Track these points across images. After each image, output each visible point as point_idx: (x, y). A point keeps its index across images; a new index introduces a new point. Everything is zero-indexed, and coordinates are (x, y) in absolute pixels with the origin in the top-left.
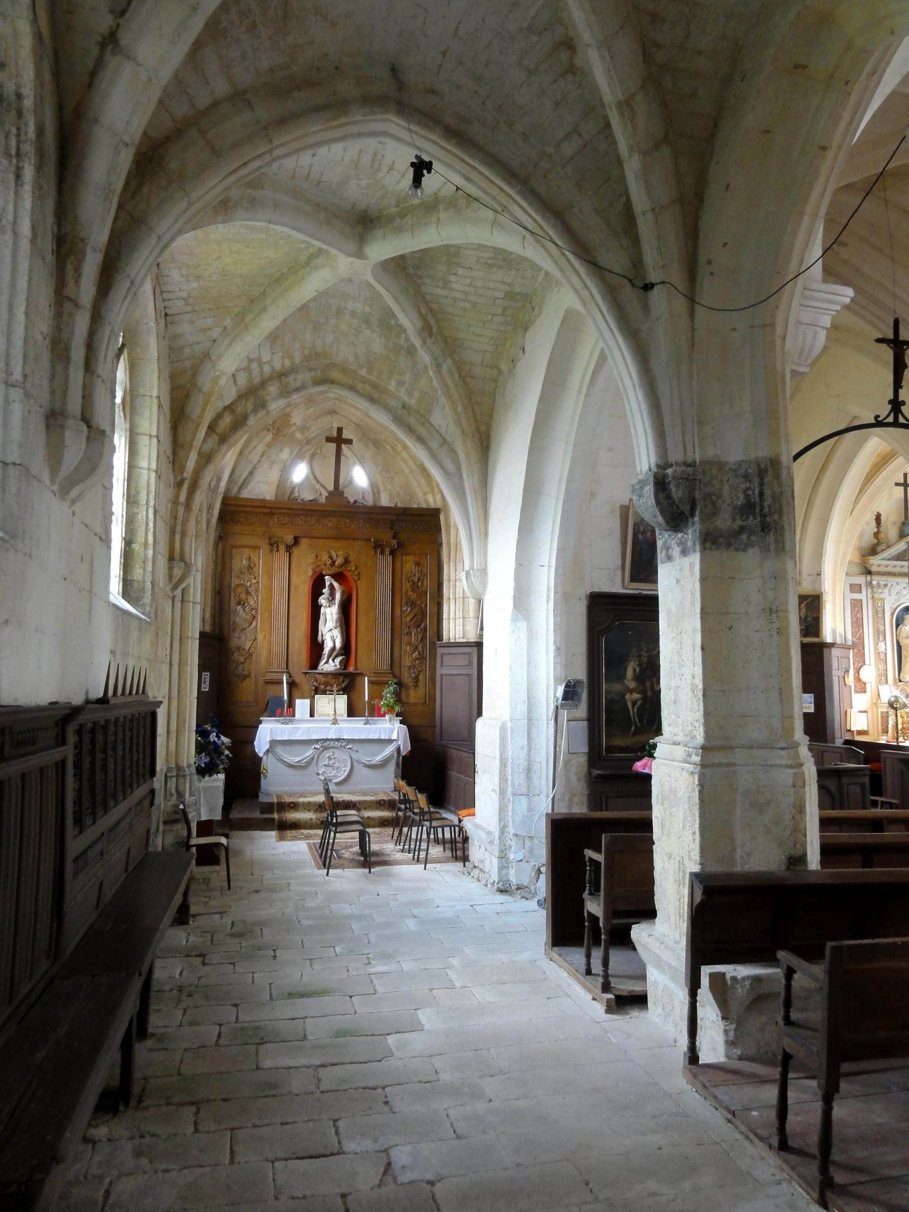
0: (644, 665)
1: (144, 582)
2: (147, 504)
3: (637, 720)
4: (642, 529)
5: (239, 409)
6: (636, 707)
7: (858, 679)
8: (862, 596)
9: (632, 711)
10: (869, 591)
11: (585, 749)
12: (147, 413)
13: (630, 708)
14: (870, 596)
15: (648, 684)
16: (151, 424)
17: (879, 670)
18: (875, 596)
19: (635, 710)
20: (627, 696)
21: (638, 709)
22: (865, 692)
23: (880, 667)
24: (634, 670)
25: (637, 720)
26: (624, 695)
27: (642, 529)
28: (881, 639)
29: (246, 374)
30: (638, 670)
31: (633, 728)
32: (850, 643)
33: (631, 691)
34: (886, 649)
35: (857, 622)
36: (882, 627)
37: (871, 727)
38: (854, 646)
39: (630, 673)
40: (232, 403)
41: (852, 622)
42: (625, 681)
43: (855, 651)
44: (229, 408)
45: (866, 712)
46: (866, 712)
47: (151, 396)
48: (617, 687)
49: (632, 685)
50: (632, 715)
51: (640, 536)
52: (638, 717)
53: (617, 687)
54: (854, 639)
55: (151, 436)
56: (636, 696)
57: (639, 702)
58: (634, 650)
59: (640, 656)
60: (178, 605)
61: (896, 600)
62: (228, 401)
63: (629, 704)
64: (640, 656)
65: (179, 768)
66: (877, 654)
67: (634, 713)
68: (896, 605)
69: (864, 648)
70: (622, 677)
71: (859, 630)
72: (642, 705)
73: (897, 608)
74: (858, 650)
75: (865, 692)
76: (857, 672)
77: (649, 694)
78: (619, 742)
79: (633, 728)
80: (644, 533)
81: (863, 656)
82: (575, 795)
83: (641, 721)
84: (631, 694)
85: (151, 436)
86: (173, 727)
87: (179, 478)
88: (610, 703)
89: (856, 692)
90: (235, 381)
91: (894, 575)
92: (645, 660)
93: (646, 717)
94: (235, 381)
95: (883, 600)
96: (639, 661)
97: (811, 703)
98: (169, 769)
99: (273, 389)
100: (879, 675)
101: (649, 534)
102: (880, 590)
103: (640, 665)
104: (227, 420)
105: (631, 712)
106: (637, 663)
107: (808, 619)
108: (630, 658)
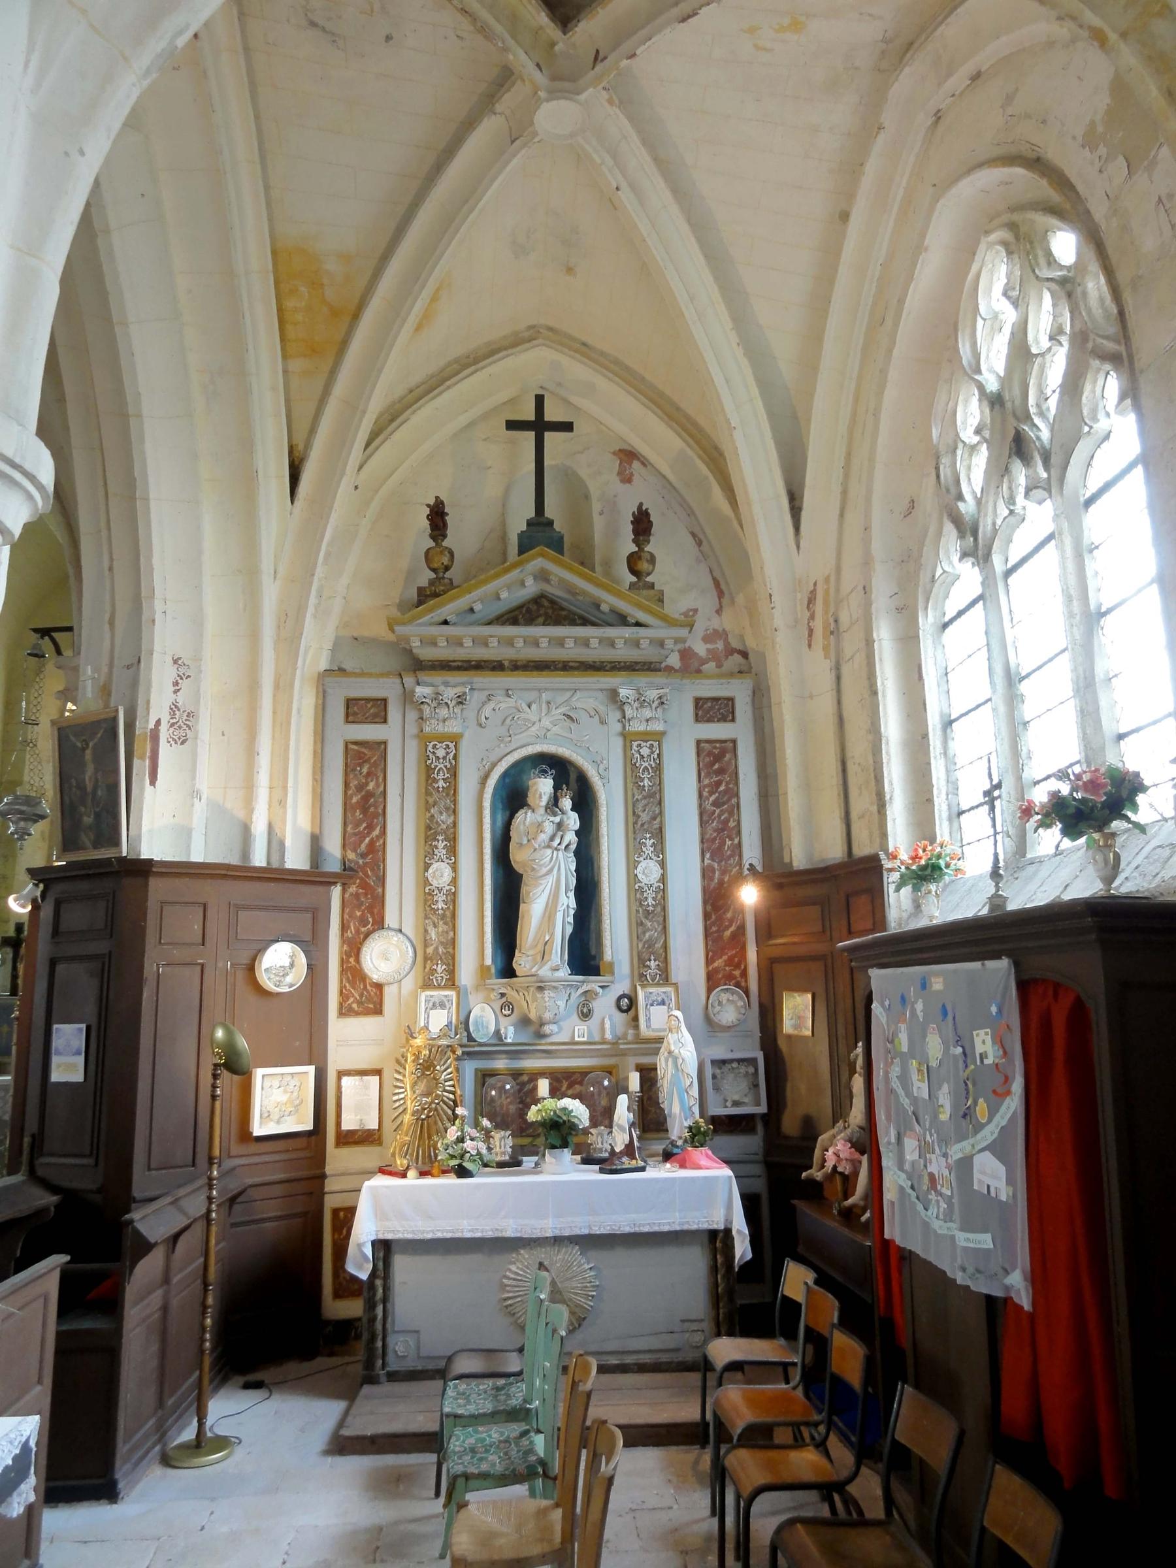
7: (353, 972)
8: (388, 732)
10: (412, 715)
14: (412, 729)
17: (426, 945)
18: (427, 729)
22: (378, 1011)
23: (433, 934)
28: (441, 851)
32: (333, 865)
34: (454, 881)
35: (364, 805)
36: (445, 819)
37: (388, 1127)
38: (348, 873)
41: (347, 807)
43: (353, 889)
45: (378, 1072)
46: (378, 1072)
54: (351, 855)
61: (500, 739)
66: (427, 895)
68: (493, 758)
69: (382, 880)
71: (370, 828)
73: (494, 765)
74: (364, 885)
75: (378, 1011)
76: (353, 949)
81: (378, 902)
89: (345, 1011)
91: (497, 667)
95: (456, 739)
97: (78, 1053)
100: (426, 958)
102: (443, 712)
107: (99, 793)
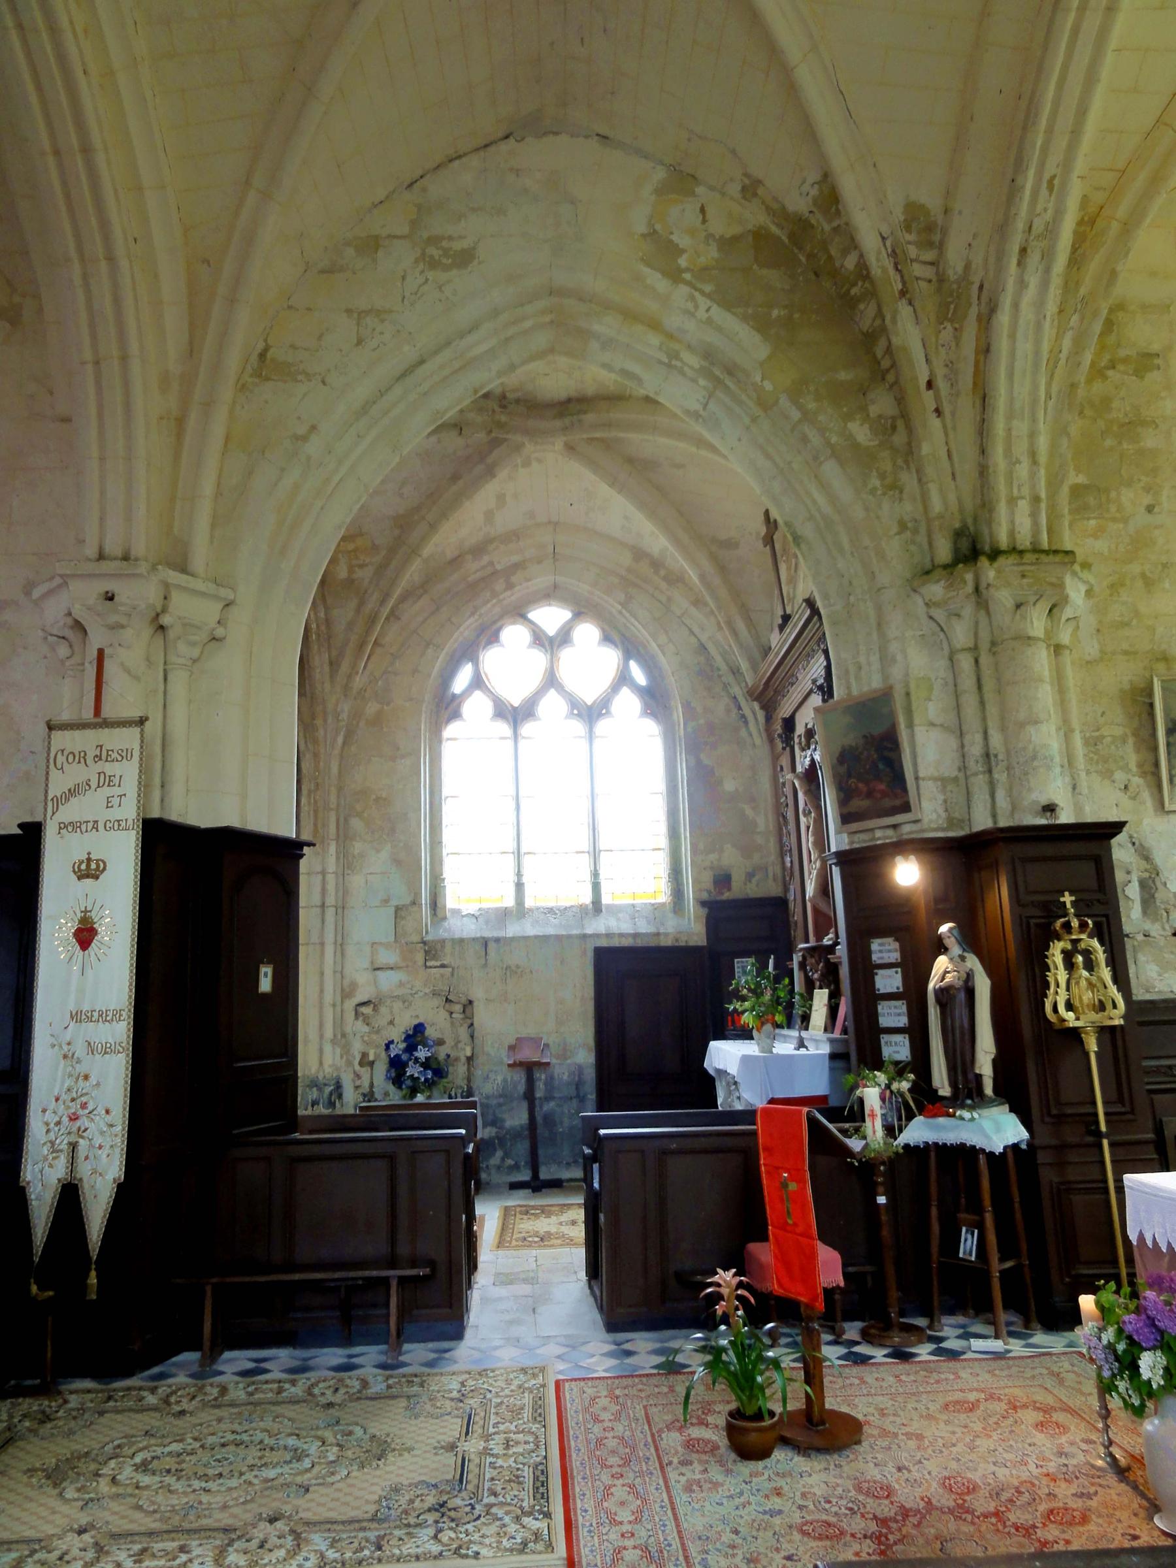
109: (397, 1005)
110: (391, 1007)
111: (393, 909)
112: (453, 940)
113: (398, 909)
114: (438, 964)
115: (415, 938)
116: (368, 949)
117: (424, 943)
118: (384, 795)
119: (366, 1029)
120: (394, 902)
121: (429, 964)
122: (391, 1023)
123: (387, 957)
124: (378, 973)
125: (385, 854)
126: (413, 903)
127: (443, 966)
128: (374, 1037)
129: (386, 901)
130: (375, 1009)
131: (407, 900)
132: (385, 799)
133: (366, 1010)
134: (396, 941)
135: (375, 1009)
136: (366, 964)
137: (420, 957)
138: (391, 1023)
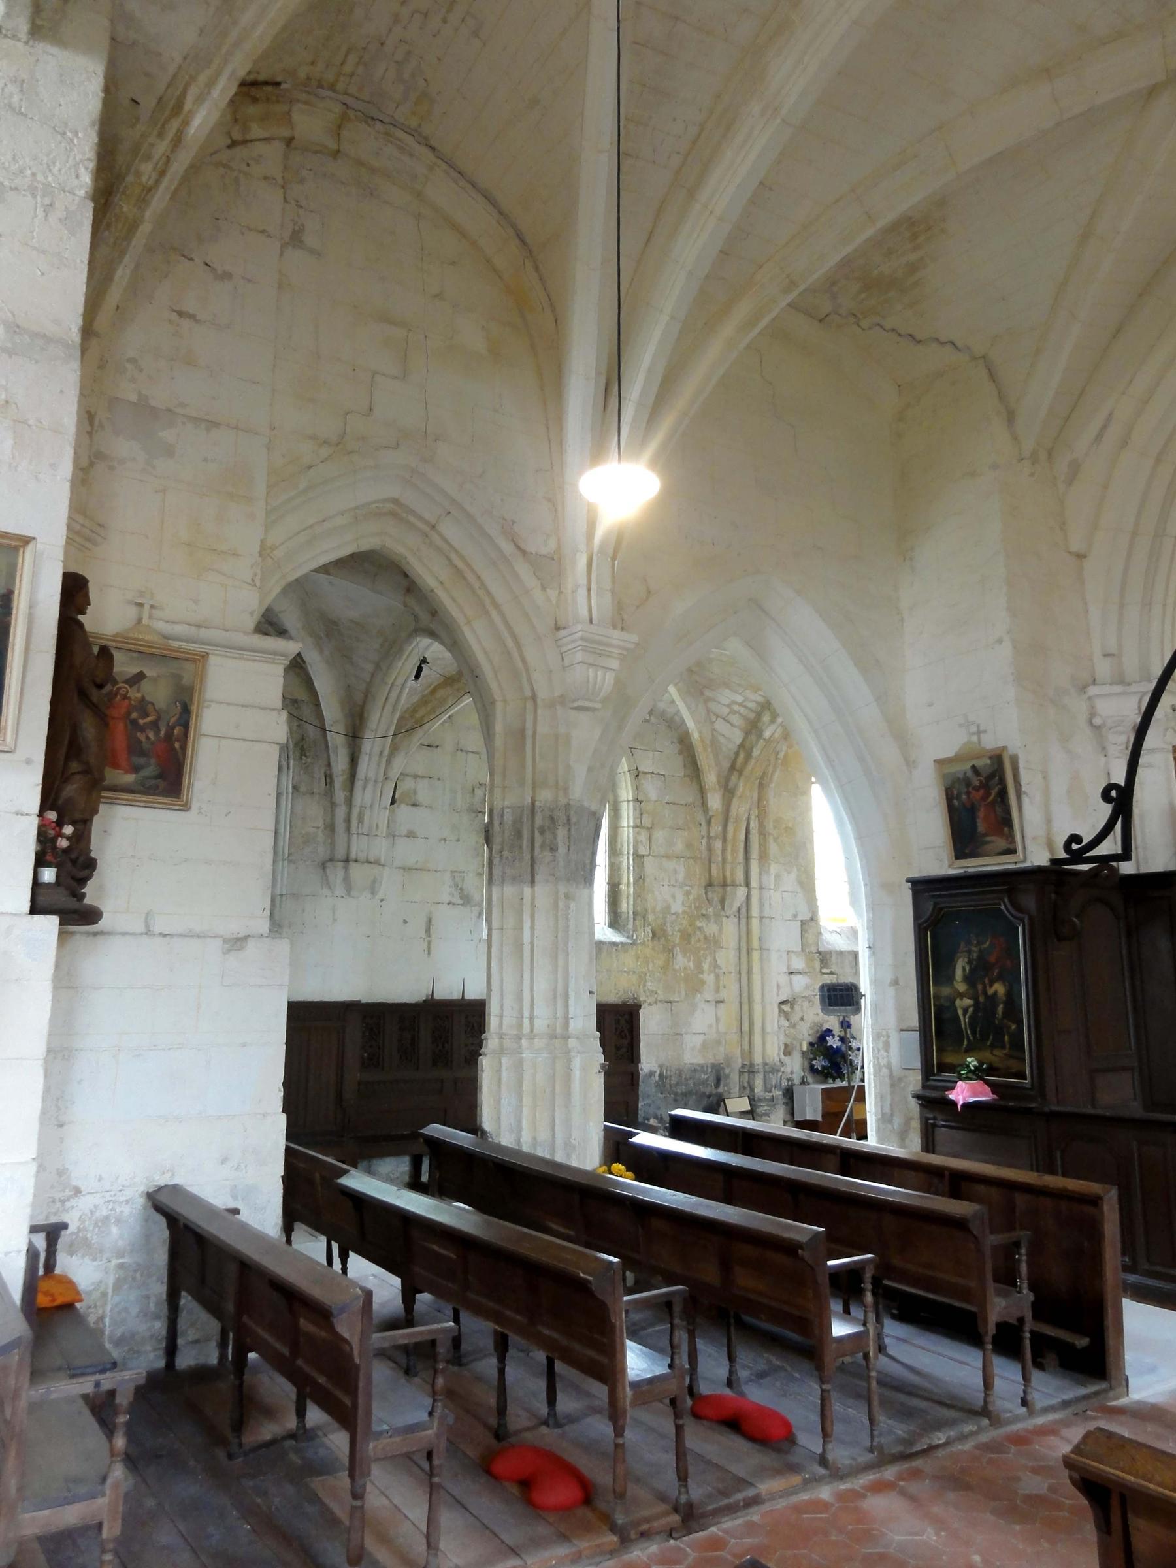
0: (974, 962)
1: (628, 913)
2: (628, 853)
3: (969, 1032)
4: (955, 792)
5: (747, 744)
6: (967, 1016)
9: (964, 1021)
11: (917, 1064)
12: (624, 785)
13: (962, 1018)
15: (980, 987)
16: (627, 792)
19: (967, 1020)
20: (958, 1002)
21: (970, 1018)
24: (964, 969)
25: (969, 1032)
26: (955, 1000)
27: (955, 792)
29: (737, 715)
30: (967, 968)
31: (965, 1042)
33: (961, 996)
39: (959, 974)
40: (743, 742)
42: (955, 983)
44: (742, 746)
47: (624, 772)
48: (946, 991)
49: (962, 987)
50: (963, 1026)
51: (956, 802)
52: (971, 1030)
53: (946, 991)
55: (628, 801)
56: (967, 1002)
57: (971, 1009)
58: (962, 944)
59: (969, 952)
60: (743, 921)
62: (738, 741)
63: (960, 1012)
64: (969, 952)
65: (752, 1065)
67: (965, 1021)
70: (950, 979)
72: (975, 1012)
77: (982, 999)
78: (950, 1059)
79: (965, 1042)
80: (958, 797)
82: (912, 1118)
83: (974, 1033)
84: (962, 999)
85: (628, 801)
86: (746, 1027)
87: (708, 817)
88: (940, 1010)
90: (732, 725)
92: (975, 955)
93: (978, 1029)
94: (732, 725)
96: (969, 958)
98: (744, 1066)
99: (766, 718)
101: (964, 797)
103: (970, 962)
104: (742, 756)
105: (962, 1023)
106: (966, 960)
108: (959, 954)
109: (806, 1004)
110: (802, 1006)
111: (799, 923)
112: (836, 951)
113: (803, 923)
114: (828, 971)
115: (814, 949)
116: (785, 955)
117: (819, 953)
118: (790, 825)
119: (787, 1024)
120: (800, 918)
121: (824, 970)
122: (802, 1019)
123: (798, 964)
124: (792, 976)
125: (793, 876)
126: (812, 919)
127: (831, 973)
128: (792, 1031)
129: (795, 916)
130: (792, 1008)
131: (807, 917)
132: (791, 829)
133: (786, 1008)
134: (803, 950)
135: (792, 1008)
136: (785, 970)
137: (817, 964)
138: (802, 1019)
